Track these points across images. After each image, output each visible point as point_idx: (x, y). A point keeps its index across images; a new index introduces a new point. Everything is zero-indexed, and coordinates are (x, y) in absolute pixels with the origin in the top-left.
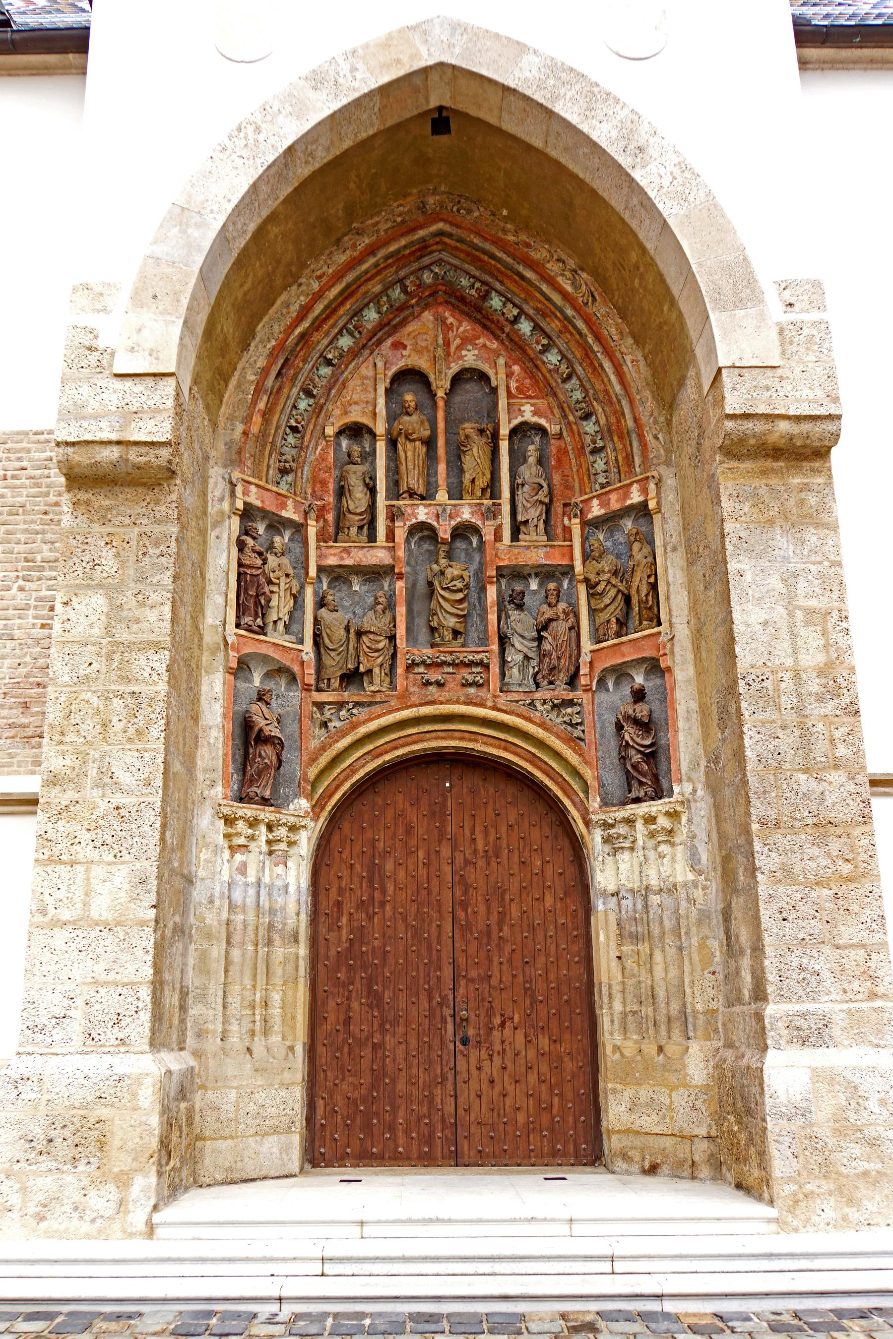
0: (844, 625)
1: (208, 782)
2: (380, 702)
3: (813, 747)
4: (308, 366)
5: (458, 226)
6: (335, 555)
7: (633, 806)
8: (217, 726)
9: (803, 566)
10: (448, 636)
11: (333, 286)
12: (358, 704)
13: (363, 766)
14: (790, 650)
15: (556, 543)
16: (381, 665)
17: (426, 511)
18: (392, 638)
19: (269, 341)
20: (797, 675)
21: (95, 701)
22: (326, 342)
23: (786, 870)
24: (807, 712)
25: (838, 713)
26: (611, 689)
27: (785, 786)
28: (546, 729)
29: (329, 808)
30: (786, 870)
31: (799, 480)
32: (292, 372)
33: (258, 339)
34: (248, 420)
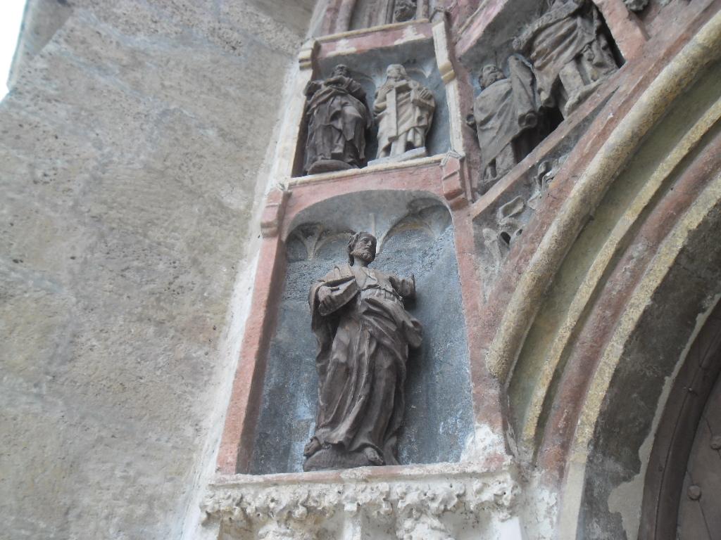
13: (636, 277)
16: (578, 58)
29: (585, 433)
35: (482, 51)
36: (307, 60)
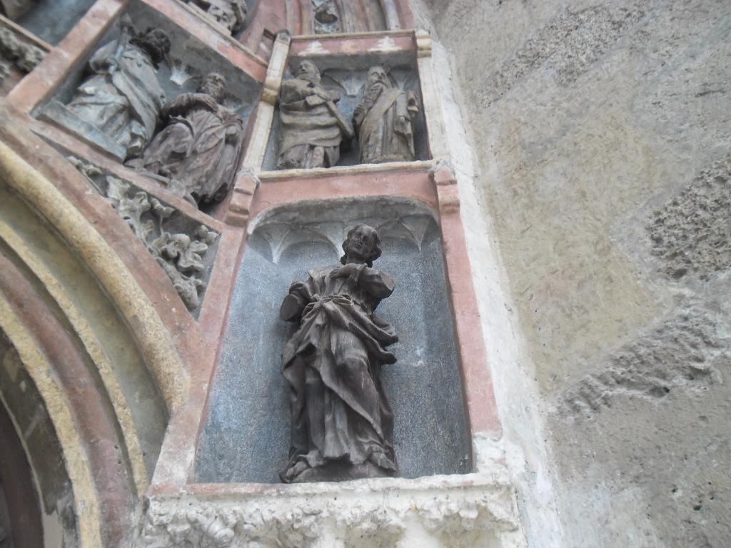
7: (323, 486)
15: (242, 46)
26: (276, 259)
28: (111, 236)
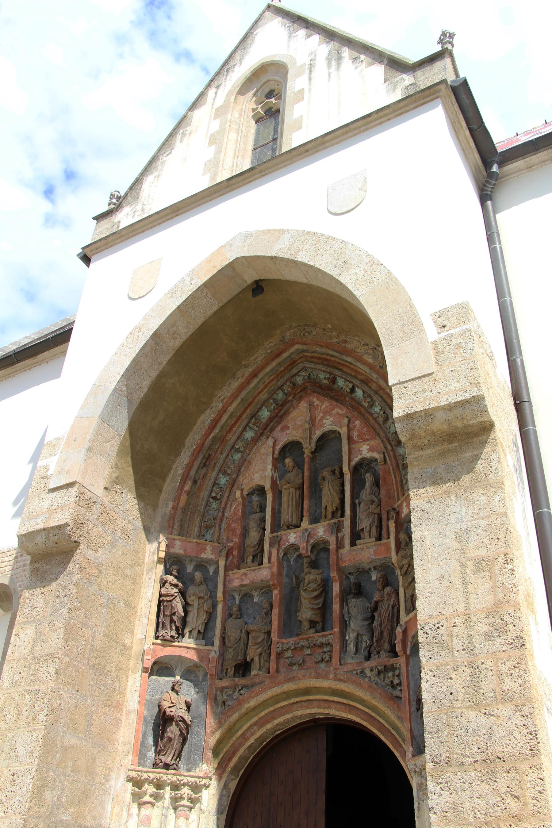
0: (510, 566)
1: (124, 753)
2: (259, 683)
3: (482, 684)
4: (224, 455)
5: (305, 344)
6: (237, 578)
8: (134, 710)
9: (473, 523)
10: (306, 624)
11: (232, 402)
12: (244, 687)
14: (462, 598)
16: (261, 655)
17: (295, 536)
18: (269, 633)
19: (192, 446)
20: (468, 619)
21: (17, 698)
22: (234, 438)
23: (456, 808)
24: (477, 651)
25: (505, 648)
27: (456, 724)
29: (229, 769)
30: (456, 808)
31: (470, 454)
32: (213, 462)
33: (186, 447)
34: (177, 499)
35: (235, 589)
36: (162, 558)
